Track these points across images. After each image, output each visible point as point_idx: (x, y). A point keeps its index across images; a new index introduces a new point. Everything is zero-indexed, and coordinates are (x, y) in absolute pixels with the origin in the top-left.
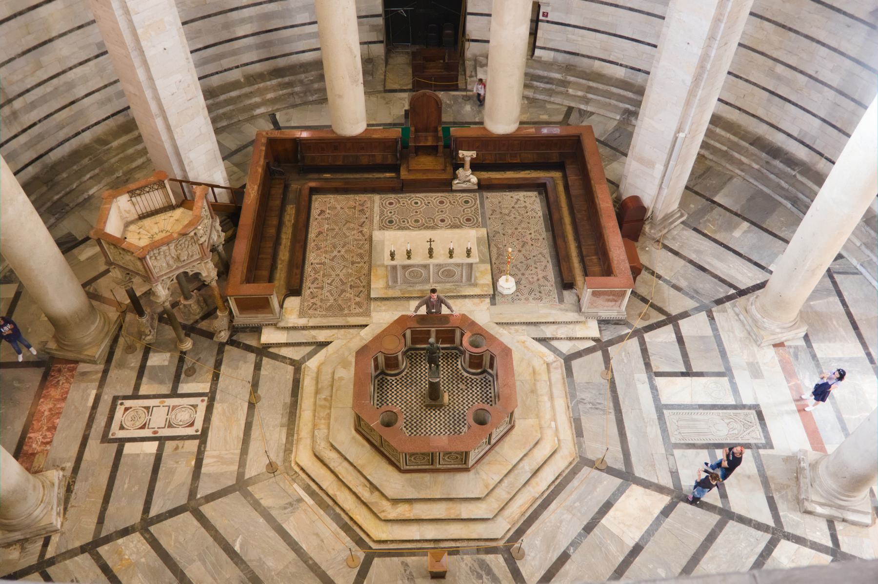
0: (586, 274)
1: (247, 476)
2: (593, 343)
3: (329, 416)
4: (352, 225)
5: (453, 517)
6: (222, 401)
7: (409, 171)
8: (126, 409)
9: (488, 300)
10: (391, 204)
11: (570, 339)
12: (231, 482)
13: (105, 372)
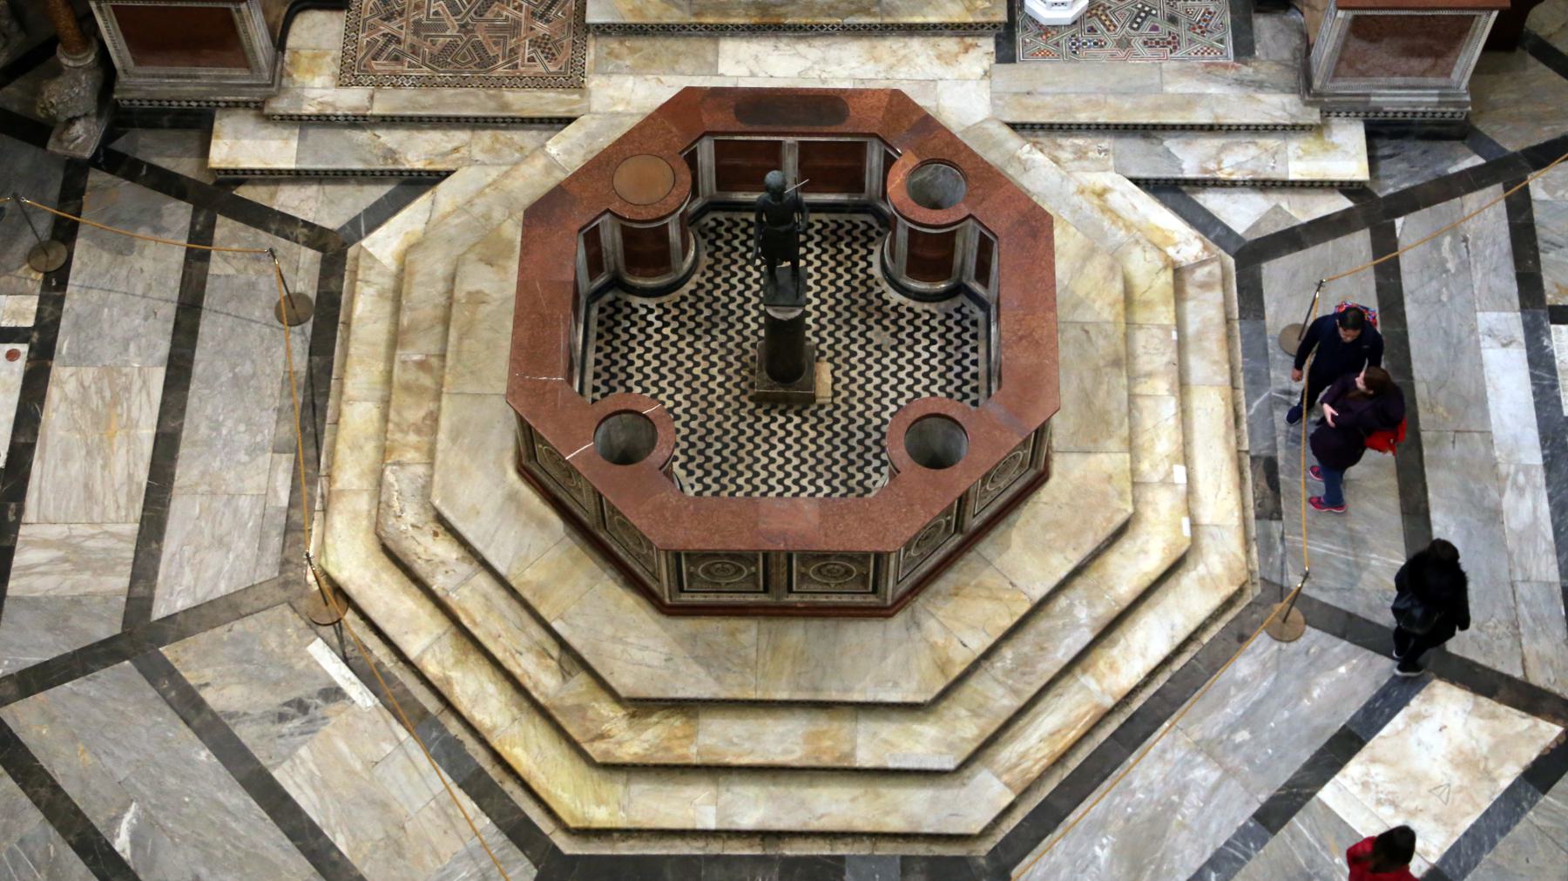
1: (159, 611)
2: (1342, 203)
5: (827, 760)
6: (78, 359)
9: (988, 44)
11: (1263, 185)
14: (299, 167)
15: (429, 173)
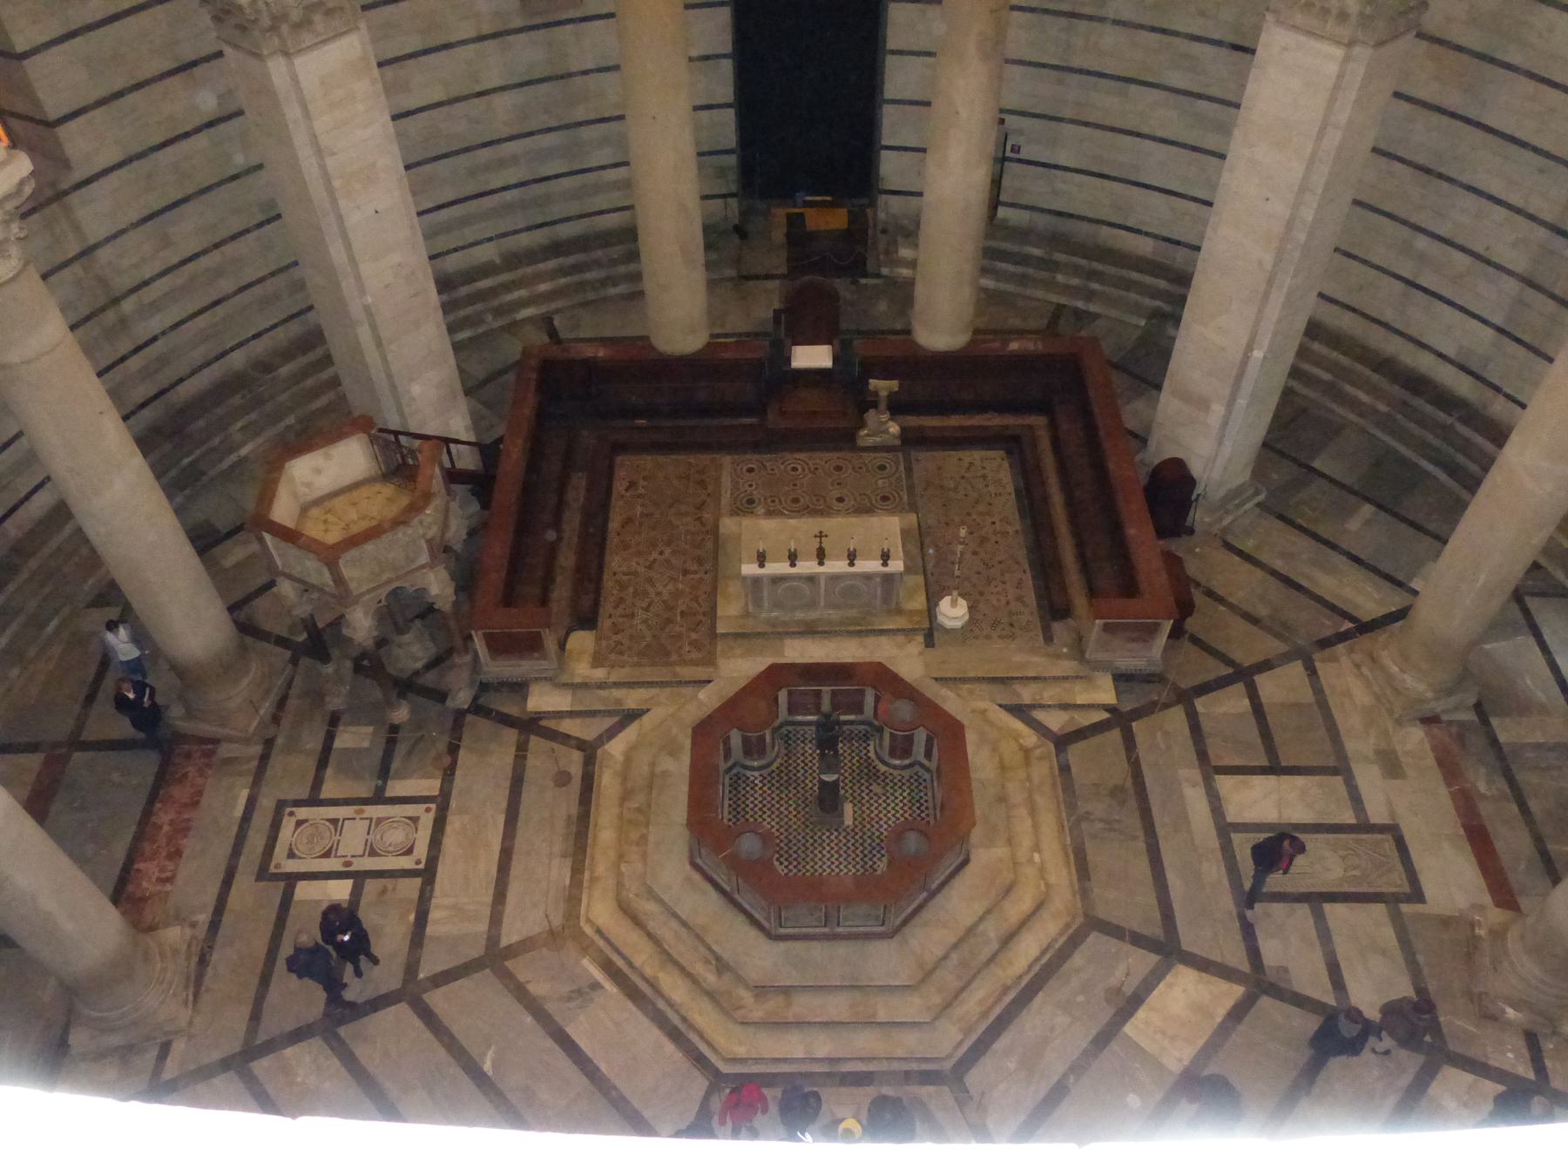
0: (1092, 592)
1: (504, 942)
2: (1105, 715)
3: (643, 839)
4: (683, 508)
8: (299, 823)
9: (920, 639)
10: (750, 470)
11: (1065, 707)
12: (476, 951)
13: (264, 758)
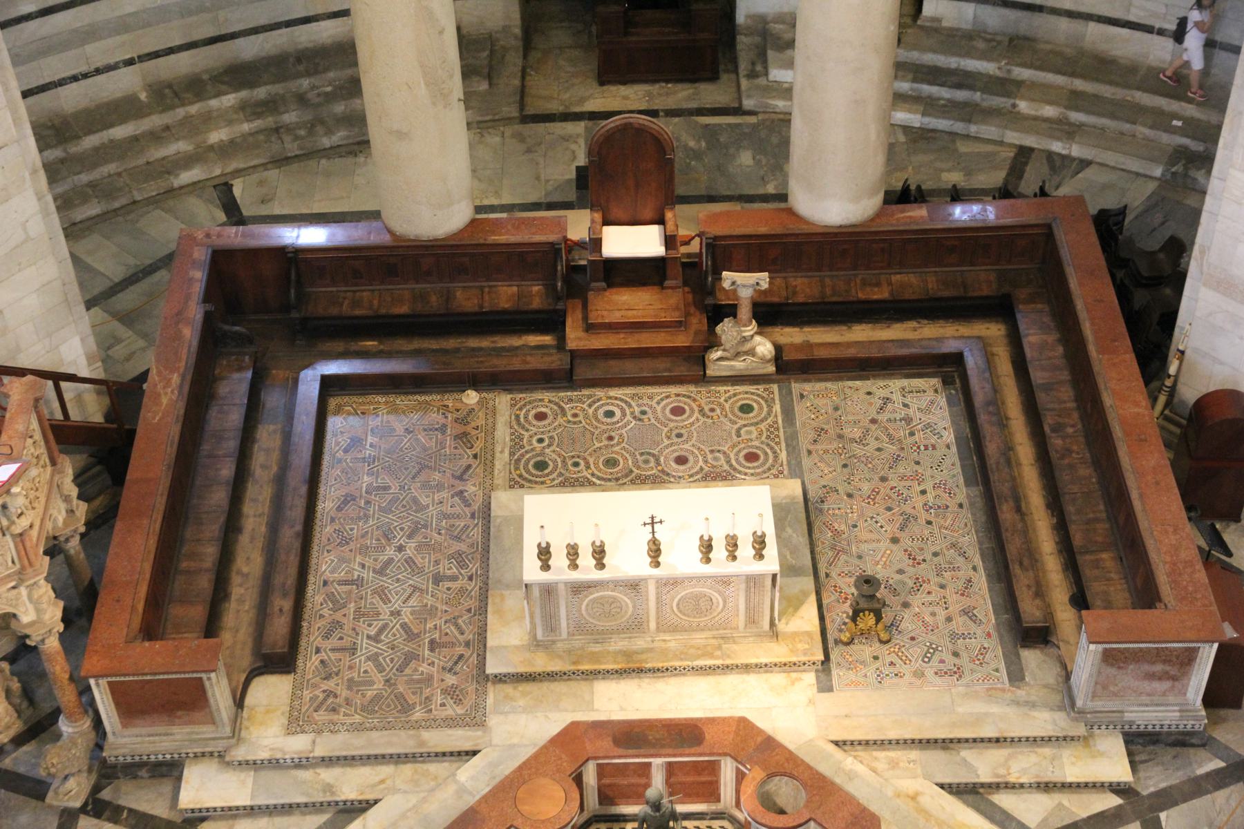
0: (1080, 601)
2: (1114, 801)
4: (437, 476)
7: (590, 328)
9: (810, 678)
10: (541, 417)
11: (1047, 787)
14: (252, 803)
15: (360, 802)
